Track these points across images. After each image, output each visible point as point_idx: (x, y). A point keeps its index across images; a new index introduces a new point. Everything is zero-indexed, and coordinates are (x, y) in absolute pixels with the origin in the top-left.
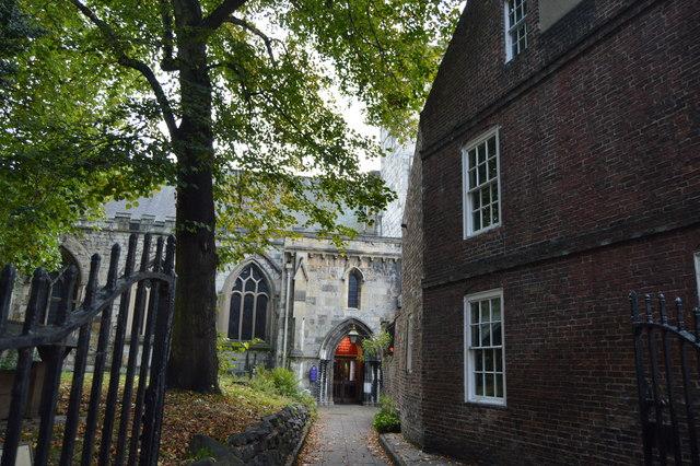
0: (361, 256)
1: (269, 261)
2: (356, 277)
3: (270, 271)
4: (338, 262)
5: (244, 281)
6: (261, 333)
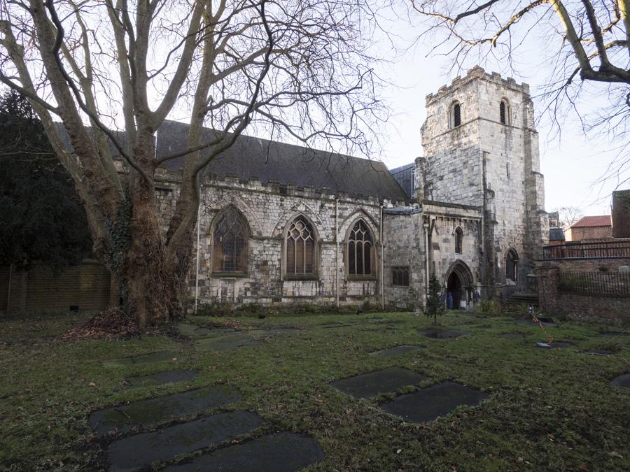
0: (462, 219)
1: (371, 218)
2: (459, 233)
3: (372, 226)
4: (450, 222)
5: (356, 233)
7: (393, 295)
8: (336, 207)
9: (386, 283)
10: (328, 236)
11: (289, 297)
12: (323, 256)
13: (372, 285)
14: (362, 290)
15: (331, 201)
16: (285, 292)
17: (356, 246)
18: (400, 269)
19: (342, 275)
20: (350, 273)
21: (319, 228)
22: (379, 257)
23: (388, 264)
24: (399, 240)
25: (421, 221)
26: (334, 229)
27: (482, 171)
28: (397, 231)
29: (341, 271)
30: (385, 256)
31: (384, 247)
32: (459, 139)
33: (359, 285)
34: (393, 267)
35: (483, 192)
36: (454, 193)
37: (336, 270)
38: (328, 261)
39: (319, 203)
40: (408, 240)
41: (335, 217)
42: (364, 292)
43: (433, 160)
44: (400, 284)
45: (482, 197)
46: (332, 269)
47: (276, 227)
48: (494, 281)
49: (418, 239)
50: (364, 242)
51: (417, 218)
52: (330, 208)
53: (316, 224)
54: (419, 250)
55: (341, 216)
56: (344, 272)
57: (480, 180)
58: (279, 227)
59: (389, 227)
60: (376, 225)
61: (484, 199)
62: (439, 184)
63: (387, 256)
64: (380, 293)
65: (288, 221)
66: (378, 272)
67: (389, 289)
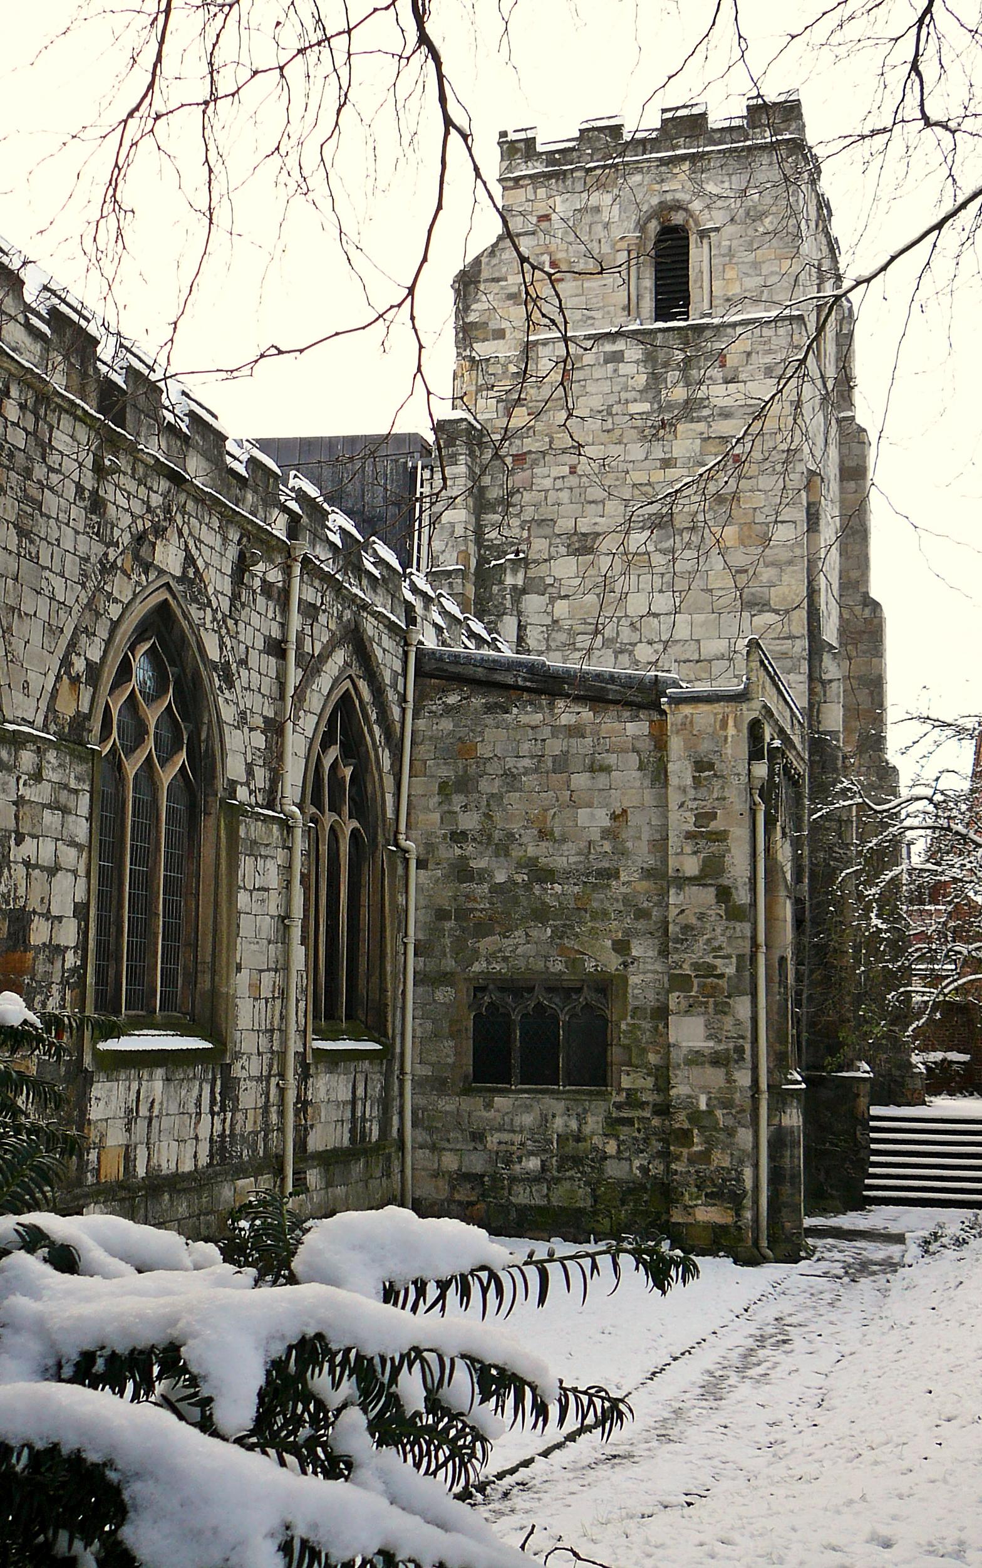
7: (478, 1137)
12: (243, 898)
23: (449, 964)
40: (607, 834)
45: (805, 667)
47: (66, 663)
49: (720, 837)
54: (724, 894)
58: (79, 665)
61: (811, 678)
63: (442, 915)
67: (447, 1104)
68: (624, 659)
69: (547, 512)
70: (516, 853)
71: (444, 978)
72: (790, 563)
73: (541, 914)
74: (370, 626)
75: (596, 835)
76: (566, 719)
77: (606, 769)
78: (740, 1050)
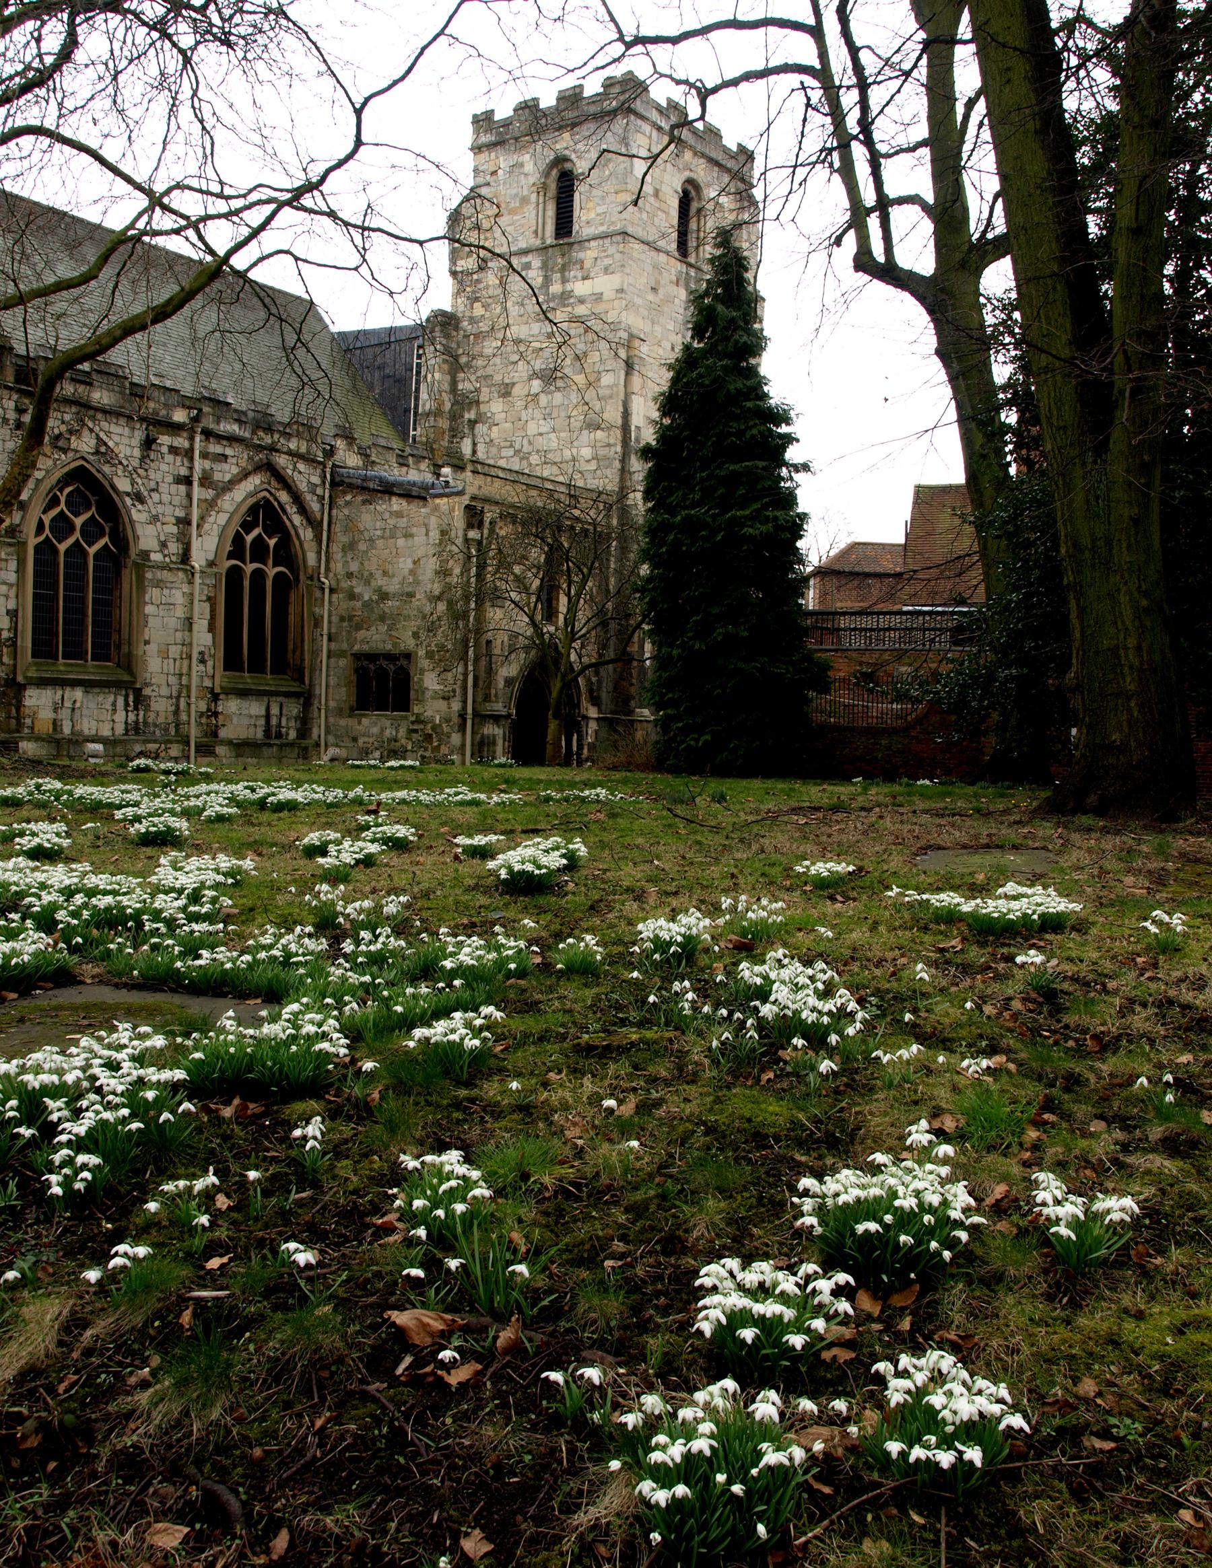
3: (297, 519)
6: (280, 667)
7: (355, 739)
8: (192, 449)
9: (332, 704)
10: (164, 545)
11: (38, 739)
12: (149, 609)
13: (293, 708)
14: (262, 722)
15: (175, 428)
16: (28, 721)
17: (247, 583)
18: (384, 663)
19: (201, 675)
20: (227, 668)
21: (138, 515)
22: (317, 623)
23: (345, 646)
24: (385, 573)
25: (458, 520)
26: (184, 522)
27: (622, 389)
28: (380, 543)
29: (202, 661)
30: (335, 619)
31: (332, 591)
32: (564, 281)
33: (256, 708)
34: (358, 656)
35: (619, 449)
36: (541, 443)
37: (190, 657)
38: (164, 627)
39: (139, 435)
40: (412, 572)
41: (188, 481)
42: (267, 731)
43: (484, 327)
44: (382, 707)
45: (617, 465)
46: (175, 651)
48: (633, 703)
50: (271, 572)
51: (452, 510)
52: (173, 450)
53: (128, 501)
55: (206, 481)
56: (210, 663)
57: (613, 414)
59: (351, 525)
60: (313, 523)
62: (496, 407)
63: (342, 619)
64: (315, 736)
65: (39, 481)
66: (312, 670)
67: (343, 722)
68: (525, 463)
69: (489, 371)
70: (373, 583)
71: (342, 654)
72: (611, 397)
73: (382, 618)
74: (282, 461)
75: (406, 572)
76: (395, 507)
77: (412, 536)
78: (454, 691)
